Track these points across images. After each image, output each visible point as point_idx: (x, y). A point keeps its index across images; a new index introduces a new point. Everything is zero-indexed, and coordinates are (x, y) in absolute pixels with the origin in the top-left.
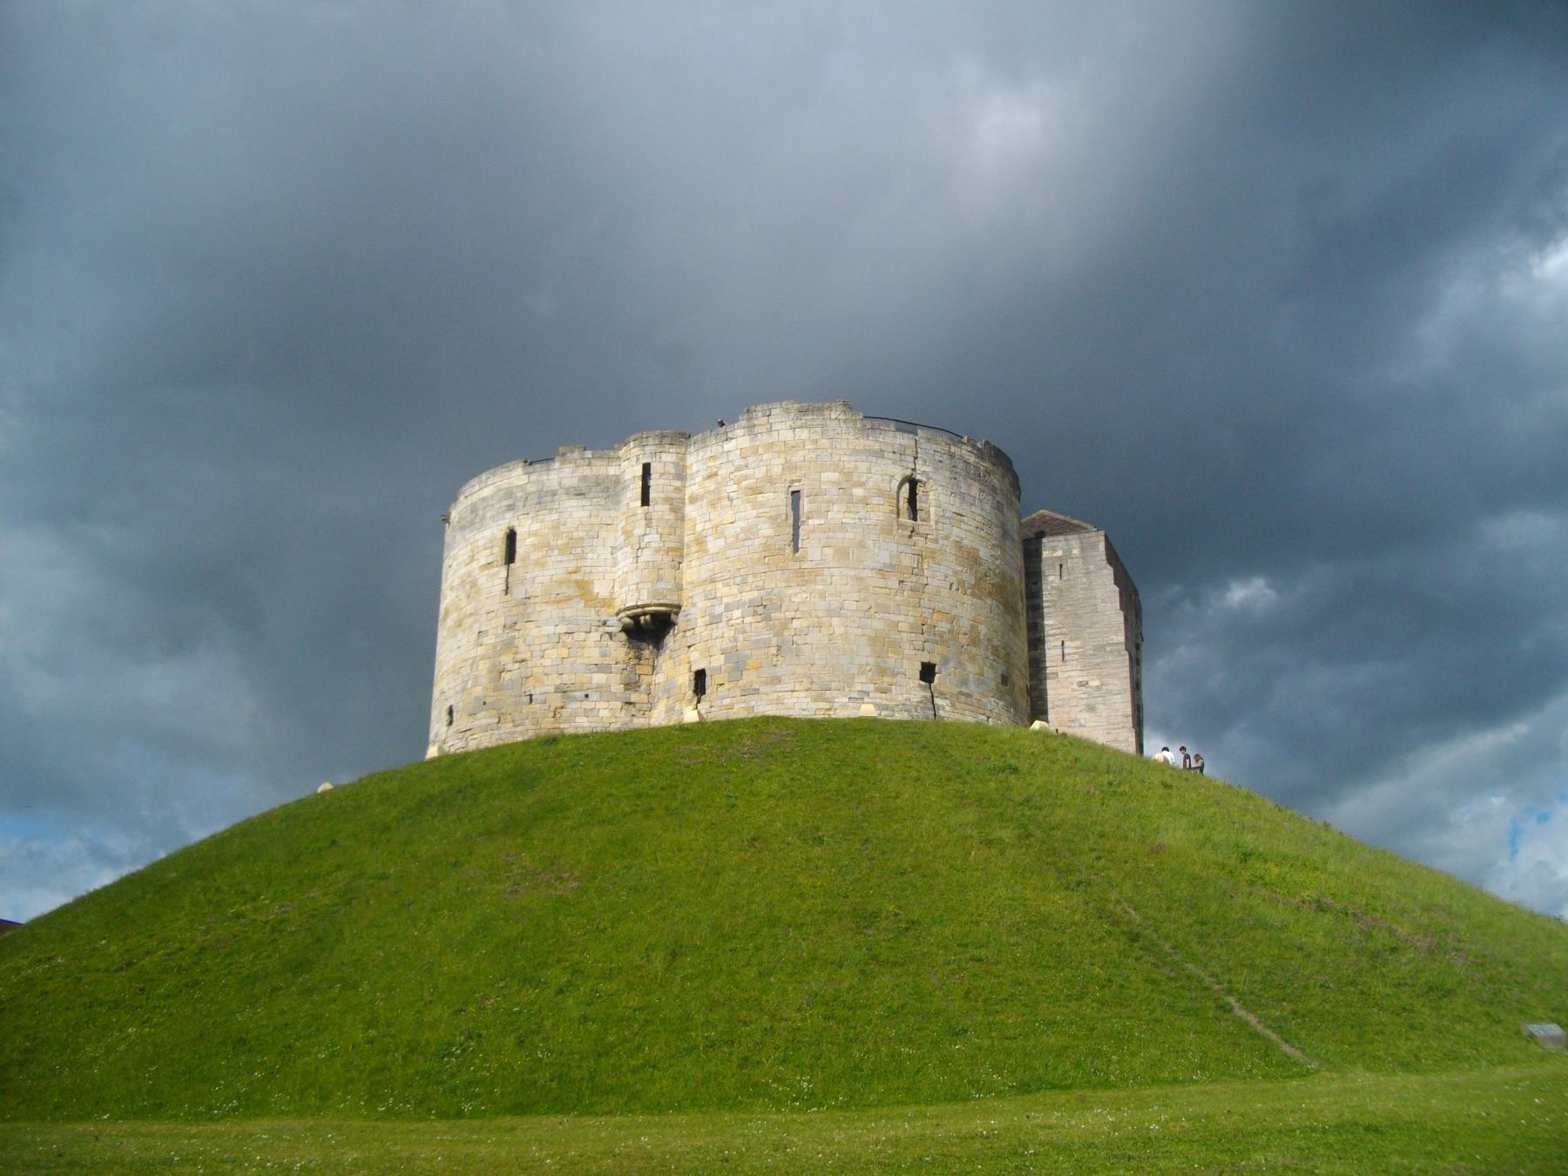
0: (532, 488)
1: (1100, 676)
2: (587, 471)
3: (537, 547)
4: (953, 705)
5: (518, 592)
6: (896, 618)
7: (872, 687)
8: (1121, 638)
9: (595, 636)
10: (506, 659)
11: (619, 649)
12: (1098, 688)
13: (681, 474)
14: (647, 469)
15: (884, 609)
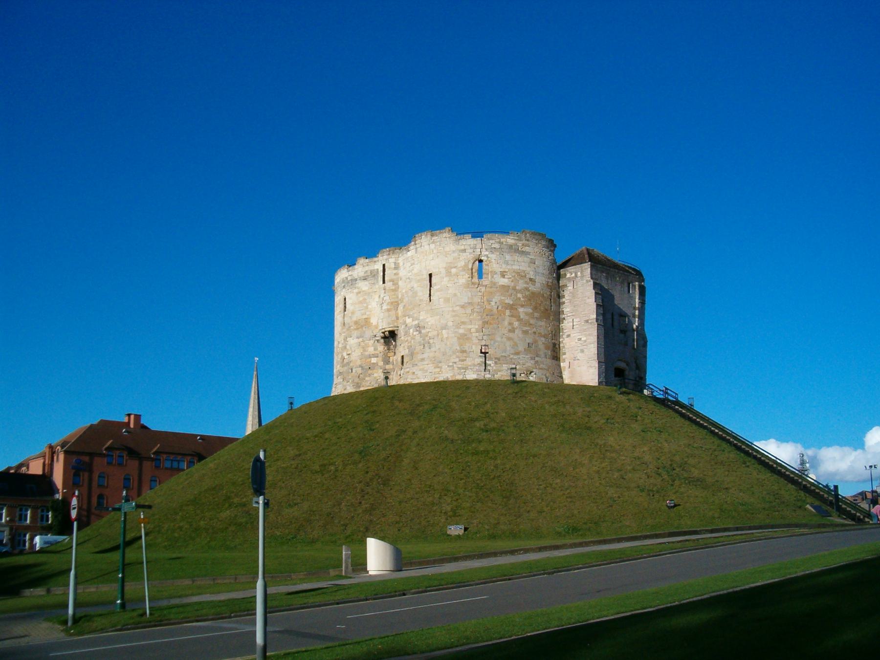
0: (349, 278)
1: (586, 336)
2: (367, 268)
3: (352, 304)
4: (496, 363)
5: (347, 326)
6: (470, 327)
7: (457, 360)
8: (595, 316)
9: (372, 342)
10: (345, 354)
11: (381, 348)
12: (585, 341)
13: (397, 267)
14: (384, 265)
15: (463, 323)
